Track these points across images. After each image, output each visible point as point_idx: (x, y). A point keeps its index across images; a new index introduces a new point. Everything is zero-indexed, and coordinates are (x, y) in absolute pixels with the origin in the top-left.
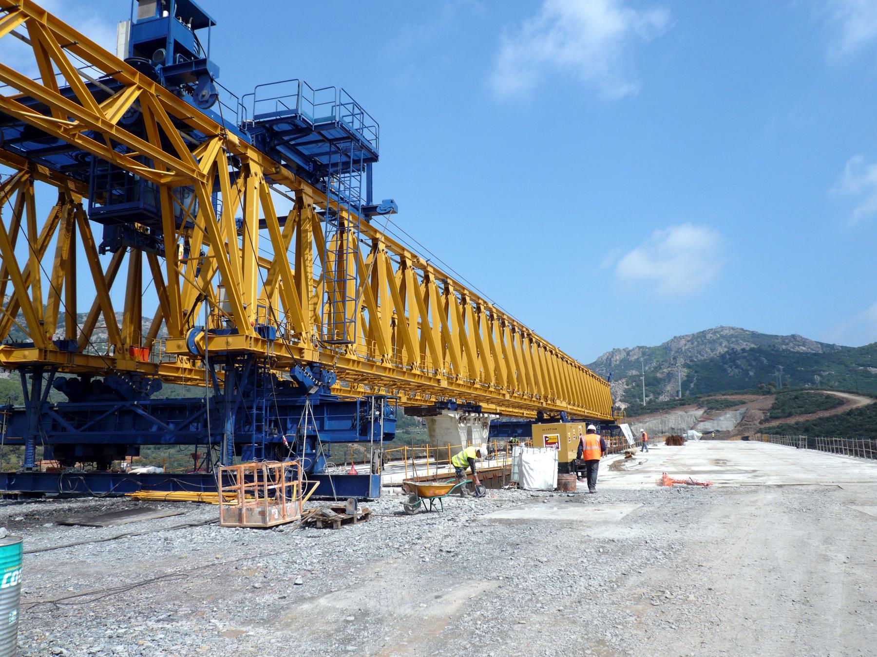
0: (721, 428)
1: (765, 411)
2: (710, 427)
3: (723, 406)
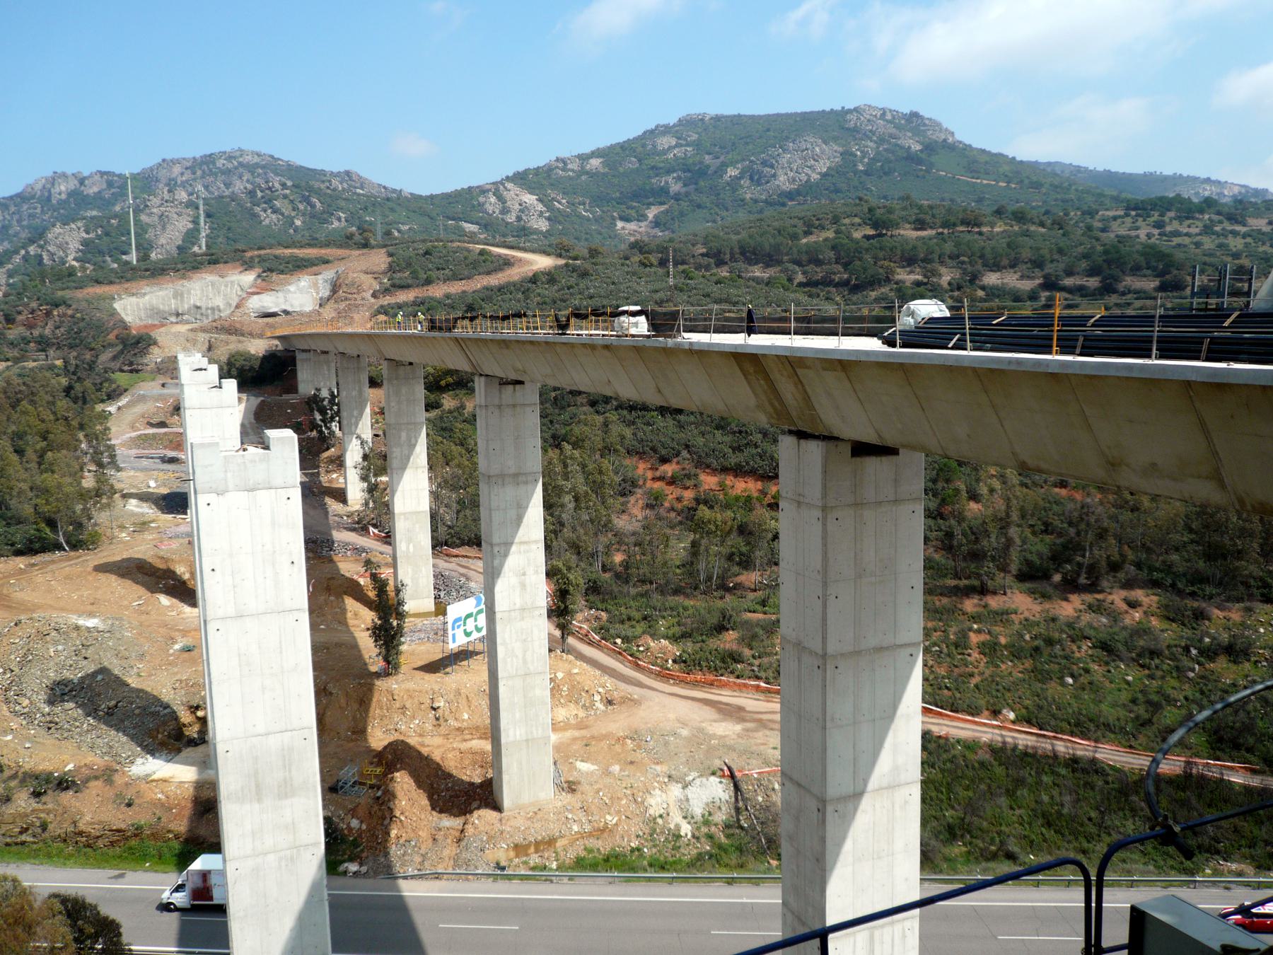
0: (292, 306)
1: (376, 276)
2: (270, 305)
3: (290, 266)
